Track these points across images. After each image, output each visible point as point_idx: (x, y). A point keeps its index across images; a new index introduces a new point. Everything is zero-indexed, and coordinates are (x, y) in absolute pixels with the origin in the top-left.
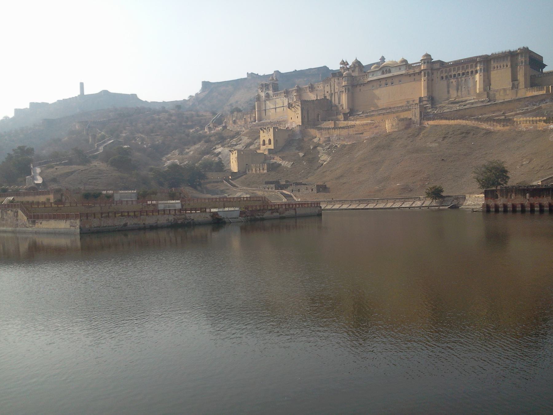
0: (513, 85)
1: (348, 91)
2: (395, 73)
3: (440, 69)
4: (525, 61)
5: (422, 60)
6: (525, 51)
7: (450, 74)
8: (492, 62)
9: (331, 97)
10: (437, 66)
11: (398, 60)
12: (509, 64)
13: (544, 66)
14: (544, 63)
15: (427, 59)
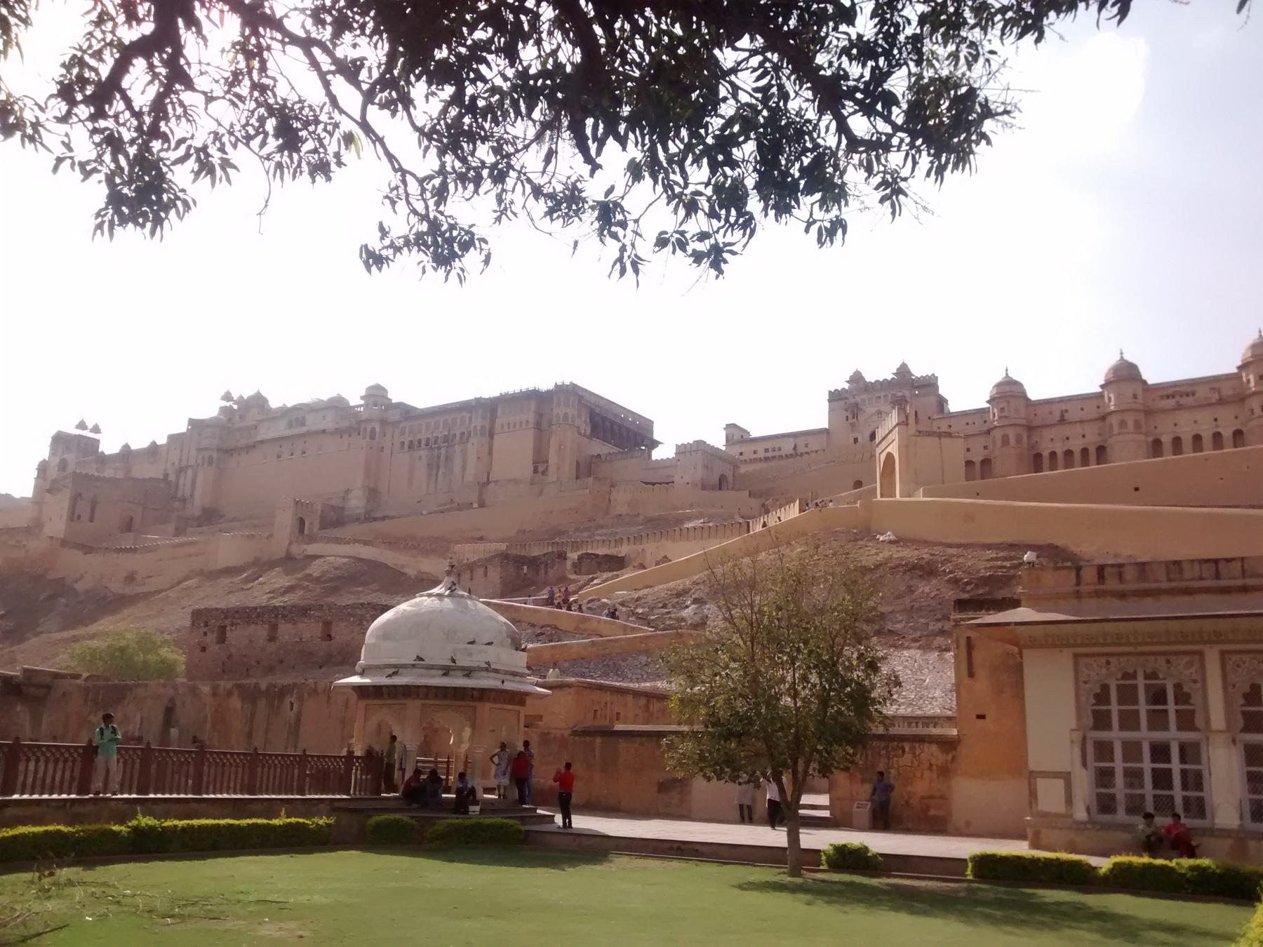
0: (536, 471)
1: (210, 464)
2: (314, 423)
3: (399, 422)
4: (566, 414)
5: (362, 398)
6: (570, 394)
7: (418, 437)
8: (499, 413)
9: (178, 477)
10: (394, 416)
11: (325, 396)
12: (531, 417)
13: (655, 444)
14: (656, 437)
15: (376, 395)
